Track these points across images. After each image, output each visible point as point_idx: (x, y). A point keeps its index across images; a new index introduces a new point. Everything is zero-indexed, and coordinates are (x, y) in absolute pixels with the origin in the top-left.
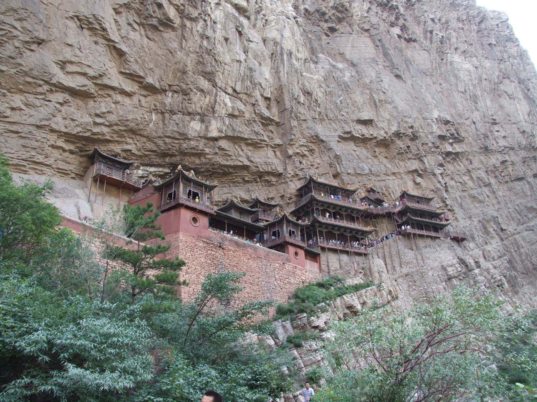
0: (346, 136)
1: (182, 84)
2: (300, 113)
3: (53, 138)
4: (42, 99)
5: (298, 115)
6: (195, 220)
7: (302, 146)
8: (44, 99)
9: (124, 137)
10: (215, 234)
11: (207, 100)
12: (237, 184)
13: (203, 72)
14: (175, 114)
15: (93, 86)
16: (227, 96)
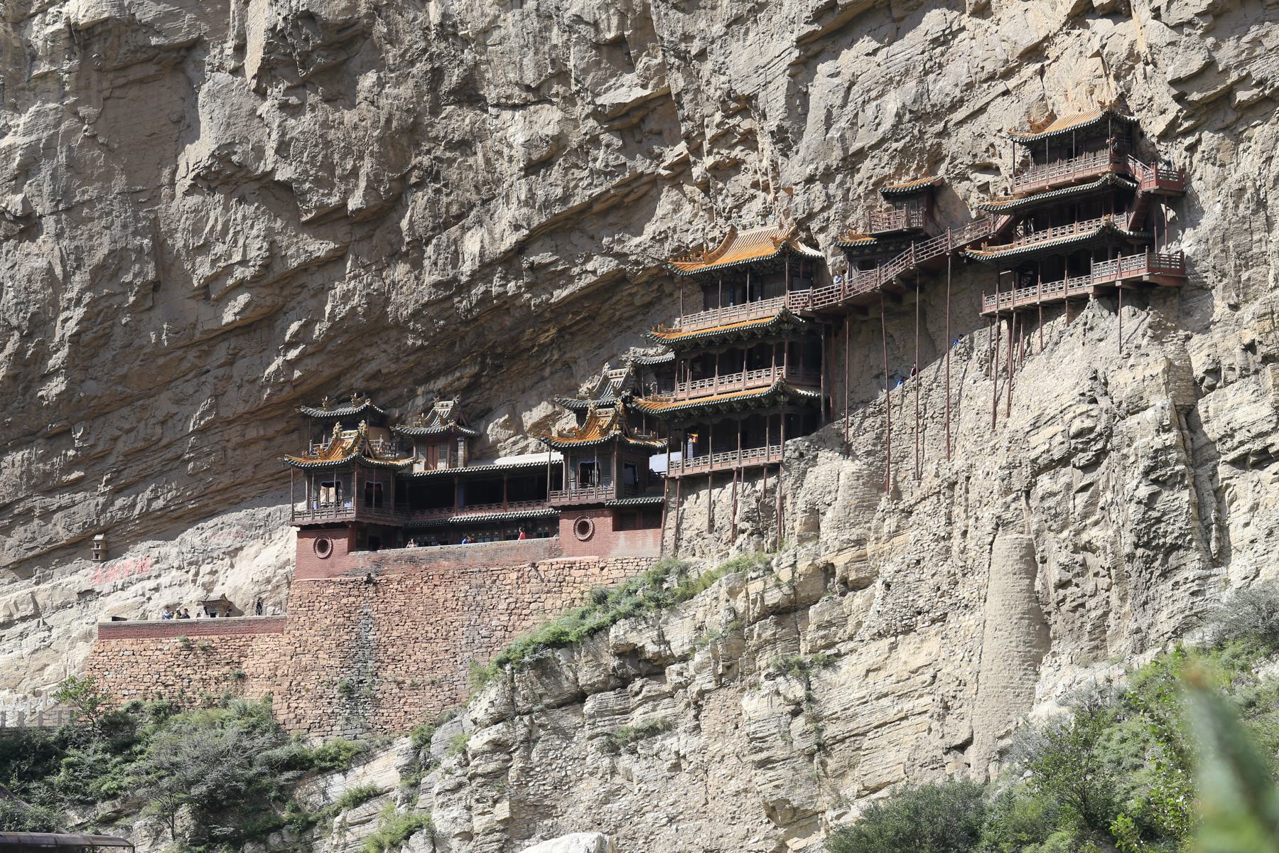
0: (831, 20)
1: (419, 158)
2: (687, 38)
3: (234, 435)
4: (195, 376)
5: (683, 46)
6: (322, 546)
7: (715, 141)
8: (195, 376)
9: (358, 350)
10: (362, 559)
11: (480, 155)
12: (625, 324)
13: (450, 93)
14: (428, 242)
15: (266, 291)
16: (518, 114)
